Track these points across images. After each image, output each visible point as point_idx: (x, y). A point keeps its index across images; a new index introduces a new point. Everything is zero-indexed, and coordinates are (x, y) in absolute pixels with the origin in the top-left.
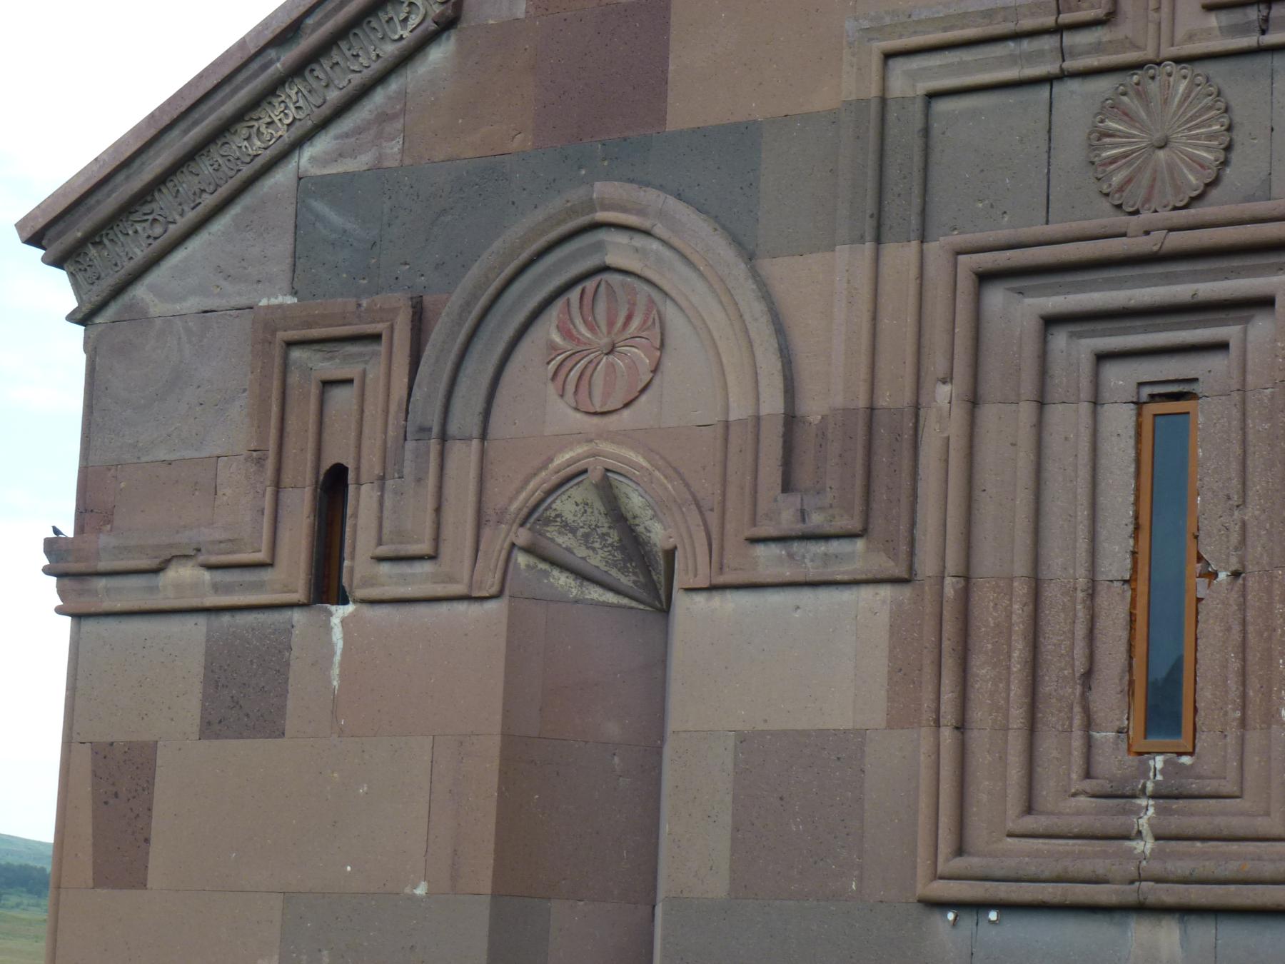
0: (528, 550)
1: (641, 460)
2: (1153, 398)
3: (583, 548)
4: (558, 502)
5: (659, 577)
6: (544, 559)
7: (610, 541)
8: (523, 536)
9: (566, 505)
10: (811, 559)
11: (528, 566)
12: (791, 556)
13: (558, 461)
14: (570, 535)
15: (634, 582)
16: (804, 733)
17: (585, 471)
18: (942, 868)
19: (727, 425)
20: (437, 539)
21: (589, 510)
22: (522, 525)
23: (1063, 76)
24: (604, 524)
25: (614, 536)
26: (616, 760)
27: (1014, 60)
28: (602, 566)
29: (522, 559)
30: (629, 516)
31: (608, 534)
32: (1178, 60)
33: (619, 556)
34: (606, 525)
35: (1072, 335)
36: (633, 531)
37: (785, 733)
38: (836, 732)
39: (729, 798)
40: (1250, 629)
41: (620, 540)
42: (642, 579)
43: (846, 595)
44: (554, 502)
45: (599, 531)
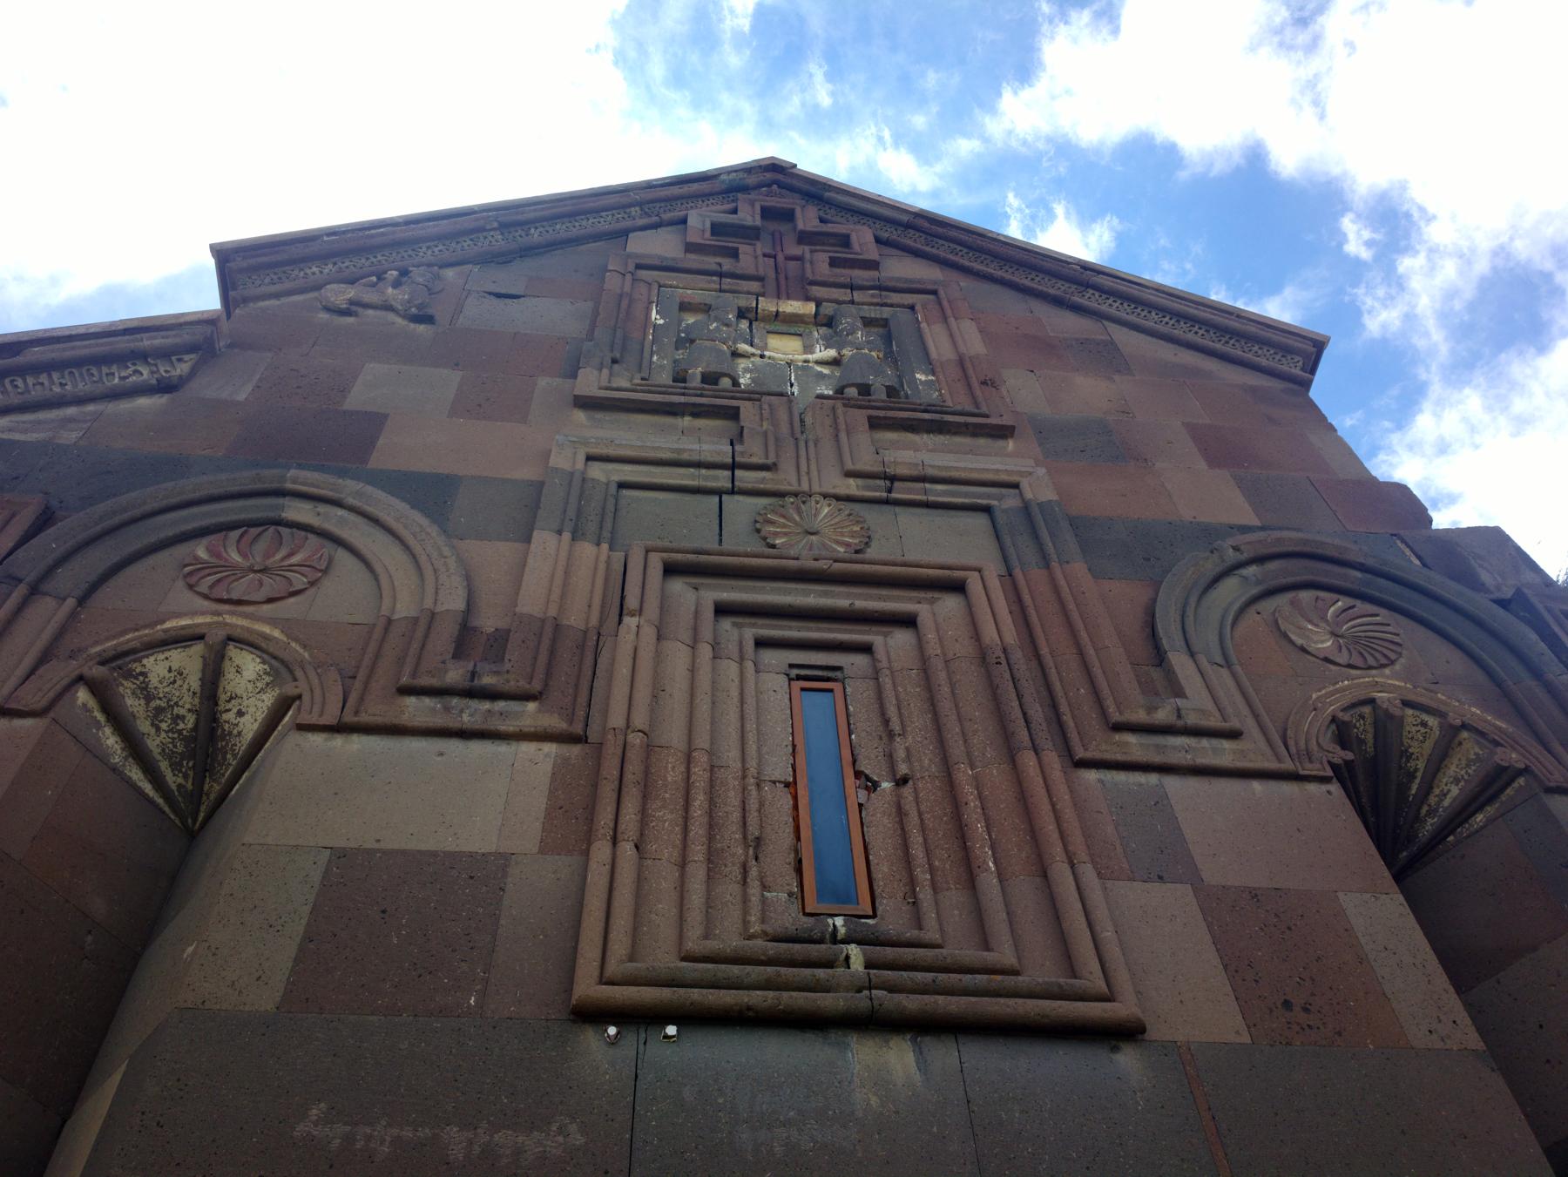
0: (96, 688)
1: (277, 633)
2: (799, 678)
3: (148, 723)
4: (152, 659)
5: (213, 788)
6: (105, 709)
7: (181, 726)
8: (98, 671)
9: (157, 667)
10: (471, 713)
11: (84, 705)
12: (447, 709)
13: (168, 625)
14: (142, 702)
15: (180, 786)
16: (434, 854)
17: (201, 637)
18: (612, 968)
19: (390, 621)
21: (179, 682)
22: (102, 663)
23: (732, 492)
24: (187, 702)
25: (191, 720)
26: (90, 938)
27: (693, 477)
28: (156, 751)
29: (83, 695)
30: (223, 697)
32: (825, 496)
33: (180, 748)
34: (188, 706)
35: (734, 624)
36: (215, 720)
37: (404, 852)
38: (471, 855)
39: (306, 910)
40: (927, 816)
41: (196, 728)
42: (190, 786)
43: (502, 748)
45: (176, 710)
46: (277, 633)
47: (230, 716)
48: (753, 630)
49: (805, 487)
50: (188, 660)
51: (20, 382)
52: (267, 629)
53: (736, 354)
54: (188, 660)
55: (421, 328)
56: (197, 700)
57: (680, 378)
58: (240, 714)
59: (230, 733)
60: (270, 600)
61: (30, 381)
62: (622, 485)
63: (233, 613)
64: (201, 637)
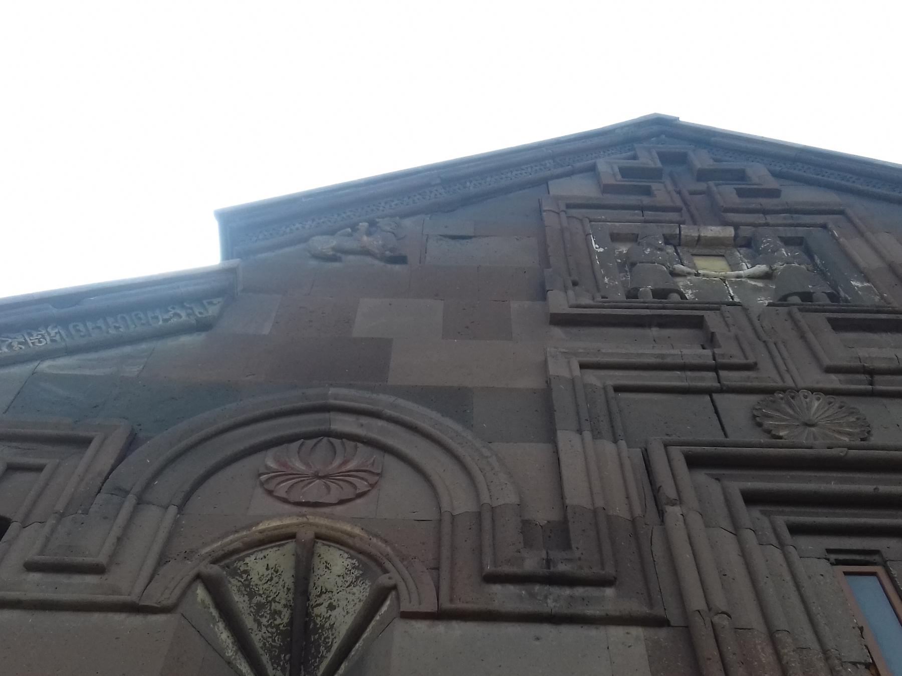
3: (251, 618)
4: (253, 557)
7: (278, 621)
9: (257, 565)
17: (292, 536)
20: (113, 556)
21: (275, 579)
24: (283, 598)
25: (286, 616)
30: (314, 592)
31: (279, 613)
33: (278, 643)
34: (283, 602)
36: (308, 614)
41: (291, 623)
44: (248, 555)
46: (357, 531)
47: (322, 610)
48: (783, 519)
49: (790, 383)
50: (280, 558)
51: (81, 327)
52: (348, 528)
53: (674, 274)
54: (280, 558)
55: (397, 268)
56: (291, 596)
57: (632, 294)
58: (331, 607)
59: (322, 627)
60: (342, 502)
61: (90, 325)
62: (618, 389)
63: (314, 514)
64: (292, 536)
